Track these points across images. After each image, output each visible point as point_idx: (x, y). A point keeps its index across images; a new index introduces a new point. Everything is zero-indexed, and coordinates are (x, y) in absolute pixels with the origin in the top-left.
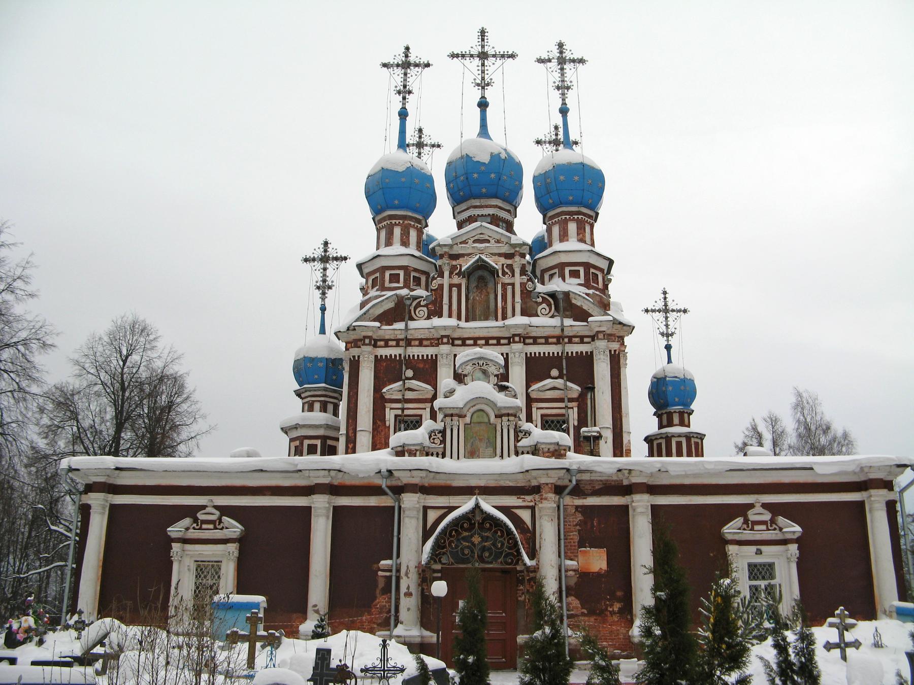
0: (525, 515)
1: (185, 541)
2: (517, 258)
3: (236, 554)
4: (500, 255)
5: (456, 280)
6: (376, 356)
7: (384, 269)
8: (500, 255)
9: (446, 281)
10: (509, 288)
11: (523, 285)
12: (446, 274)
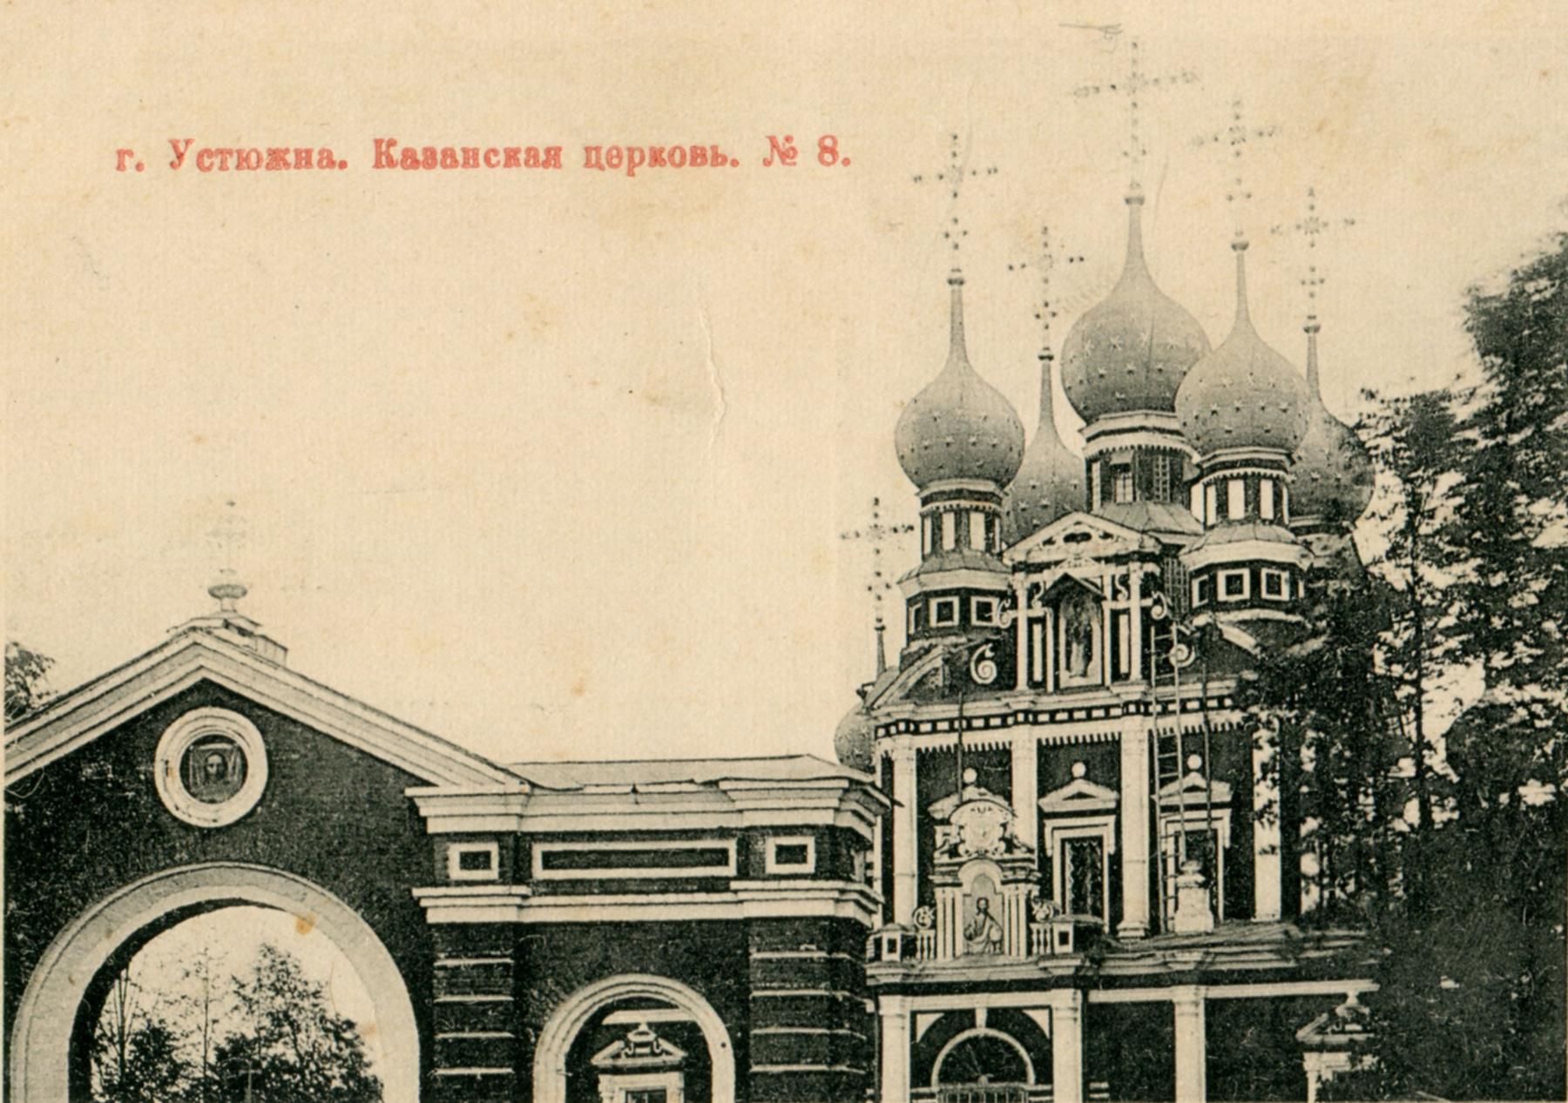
0: (1040, 1018)
1: (616, 1071)
2: (1134, 566)
3: (681, 1085)
4: (1108, 560)
5: (1038, 610)
6: (919, 750)
7: (927, 596)
8: (1108, 560)
9: (1022, 615)
10: (1123, 619)
11: (1145, 612)
12: (1022, 601)
